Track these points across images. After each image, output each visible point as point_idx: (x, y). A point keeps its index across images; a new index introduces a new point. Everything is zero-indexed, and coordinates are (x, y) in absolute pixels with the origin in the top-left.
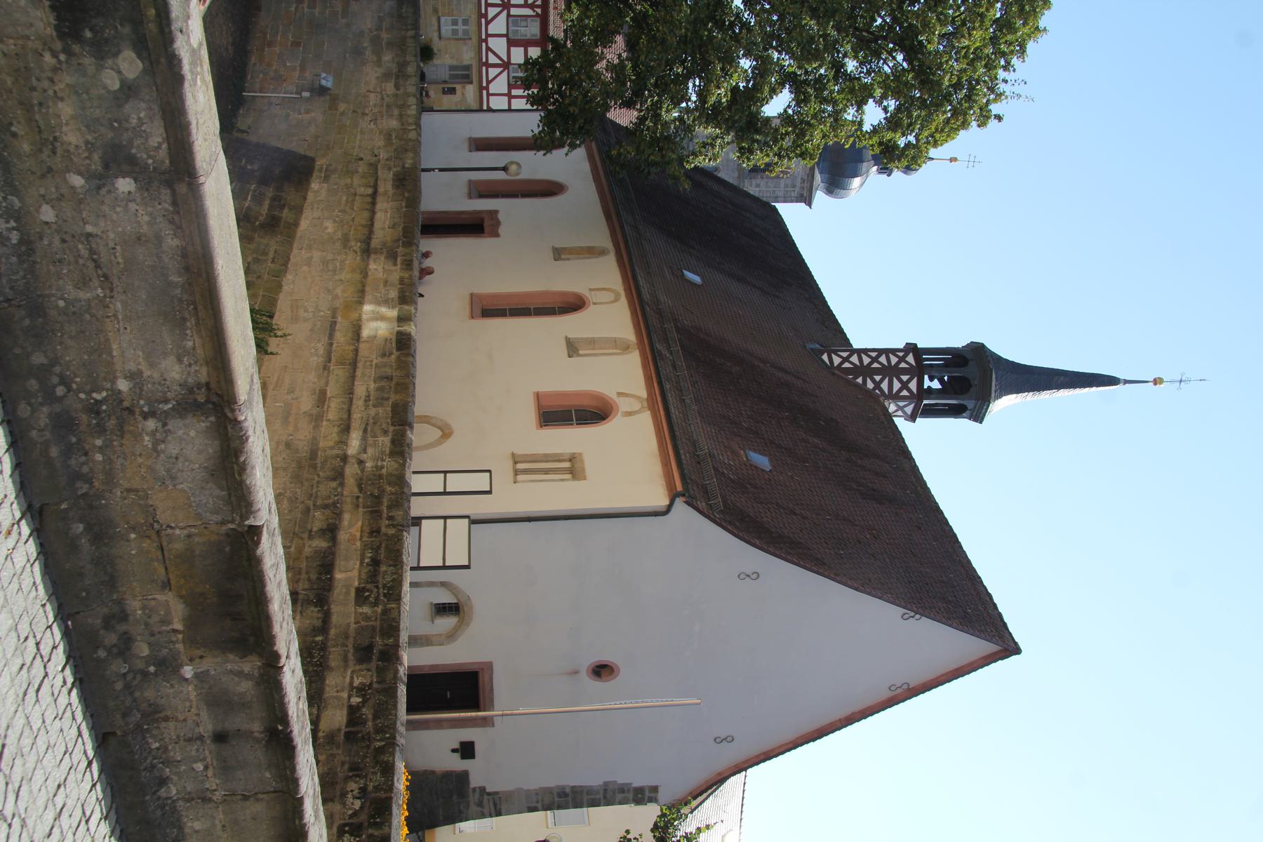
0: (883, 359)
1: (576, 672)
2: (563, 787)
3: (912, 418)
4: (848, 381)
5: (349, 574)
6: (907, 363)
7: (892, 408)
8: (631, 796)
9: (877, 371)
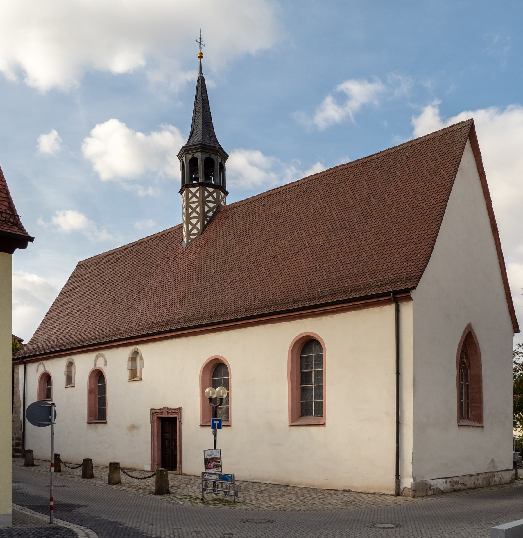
0: (194, 205)
4: (207, 224)
6: (196, 192)
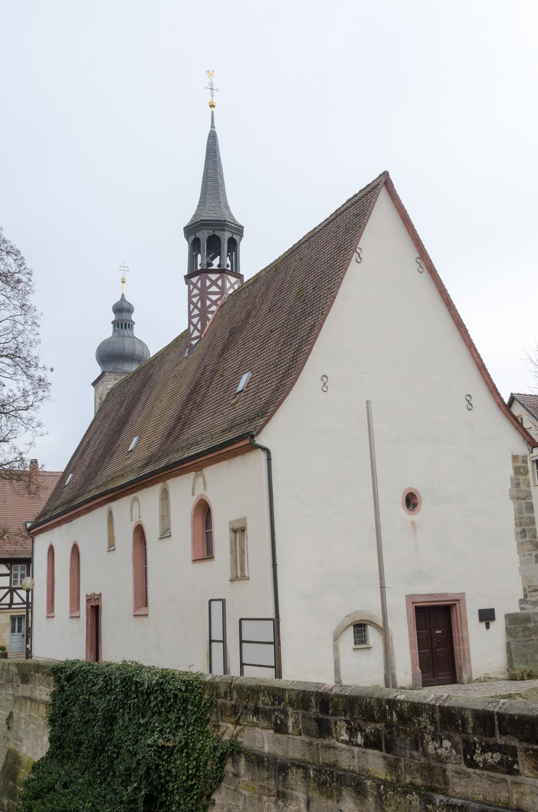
0: (195, 300)
1: (413, 523)
2: (517, 533)
3: (240, 277)
5: (265, 738)
7: (231, 291)
8: (522, 478)
9: (203, 302)
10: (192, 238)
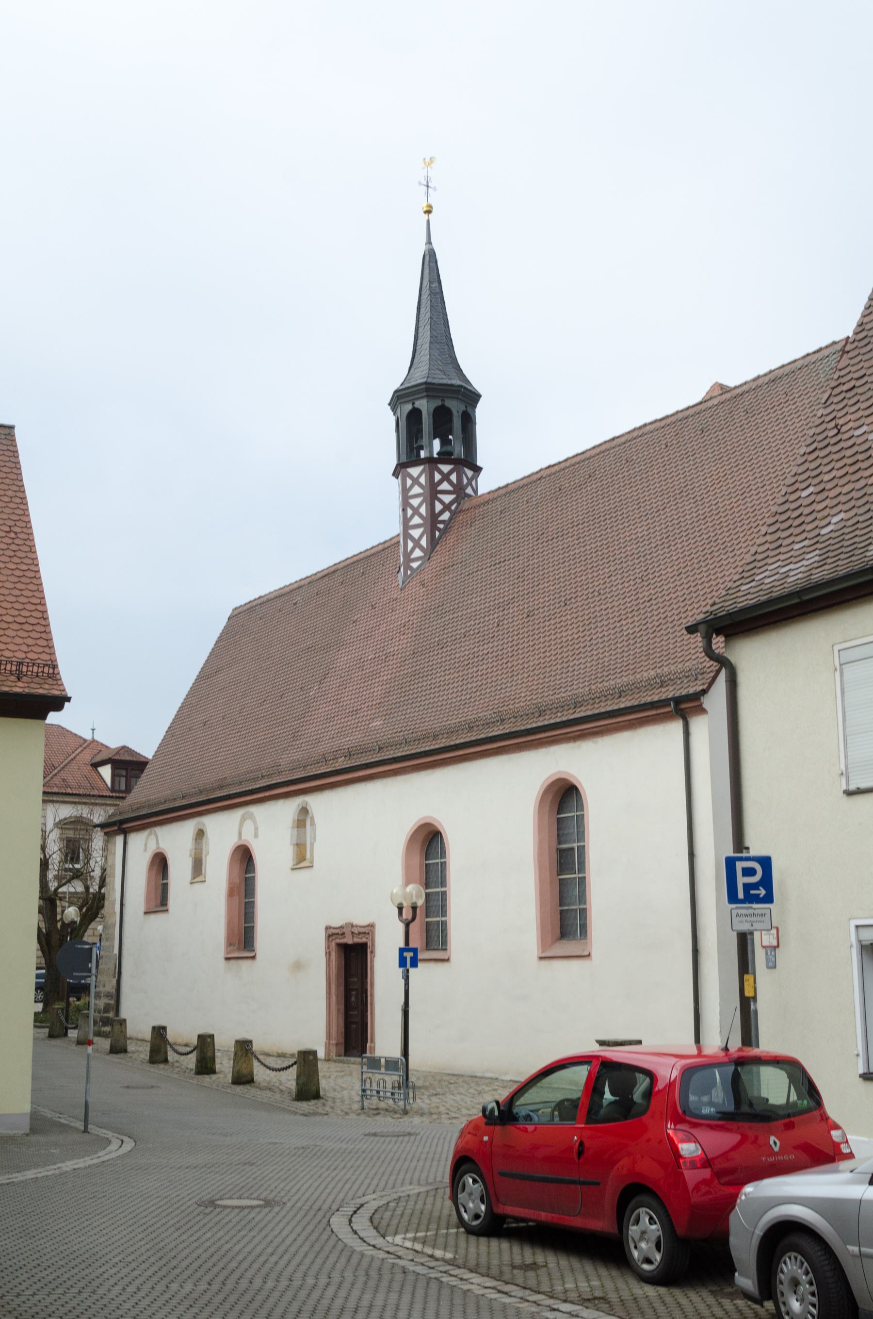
0: (415, 502)
6: (420, 475)
10: (408, 407)
